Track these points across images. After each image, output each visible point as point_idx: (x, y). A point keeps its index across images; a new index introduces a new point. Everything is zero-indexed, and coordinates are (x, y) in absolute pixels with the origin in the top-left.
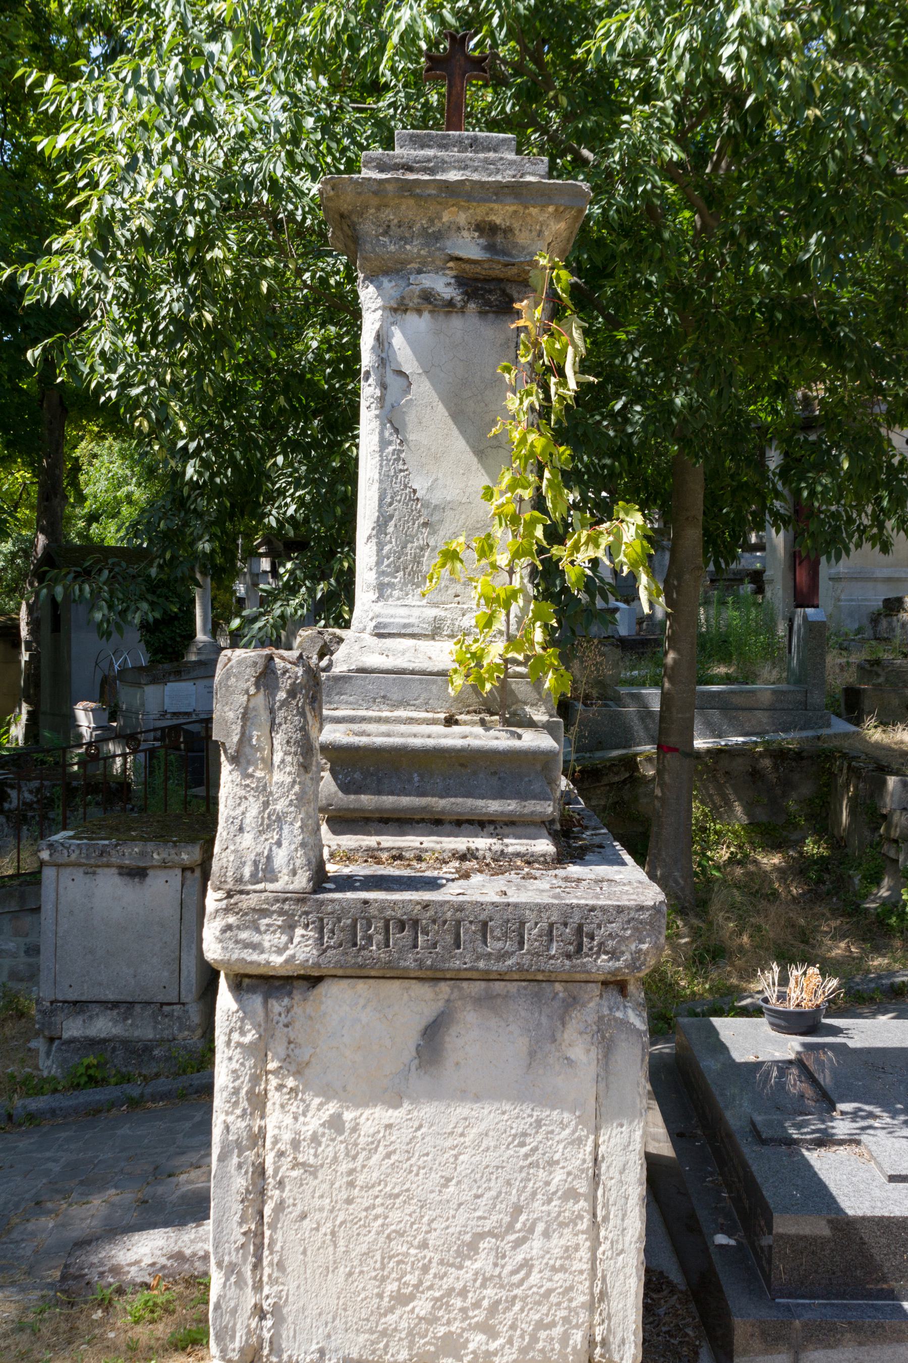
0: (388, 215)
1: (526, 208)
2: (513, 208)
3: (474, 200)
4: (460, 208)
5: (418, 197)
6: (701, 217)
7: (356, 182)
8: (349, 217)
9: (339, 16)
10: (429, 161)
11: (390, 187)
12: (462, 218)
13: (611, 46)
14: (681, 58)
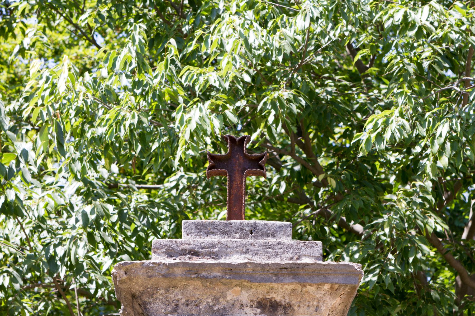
0: (177, 295)
1: (304, 286)
2: (291, 287)
3: (256, 280)
4: (243, 287)
5: (205, 279)
6: (462, 279)
7: (148, 267)
8: (140, 297)
9: (133, 117)
10: (214, 246)
11: (178, 271)
12: (245, 297)
13: (380, 137)
14: (442, 147)
